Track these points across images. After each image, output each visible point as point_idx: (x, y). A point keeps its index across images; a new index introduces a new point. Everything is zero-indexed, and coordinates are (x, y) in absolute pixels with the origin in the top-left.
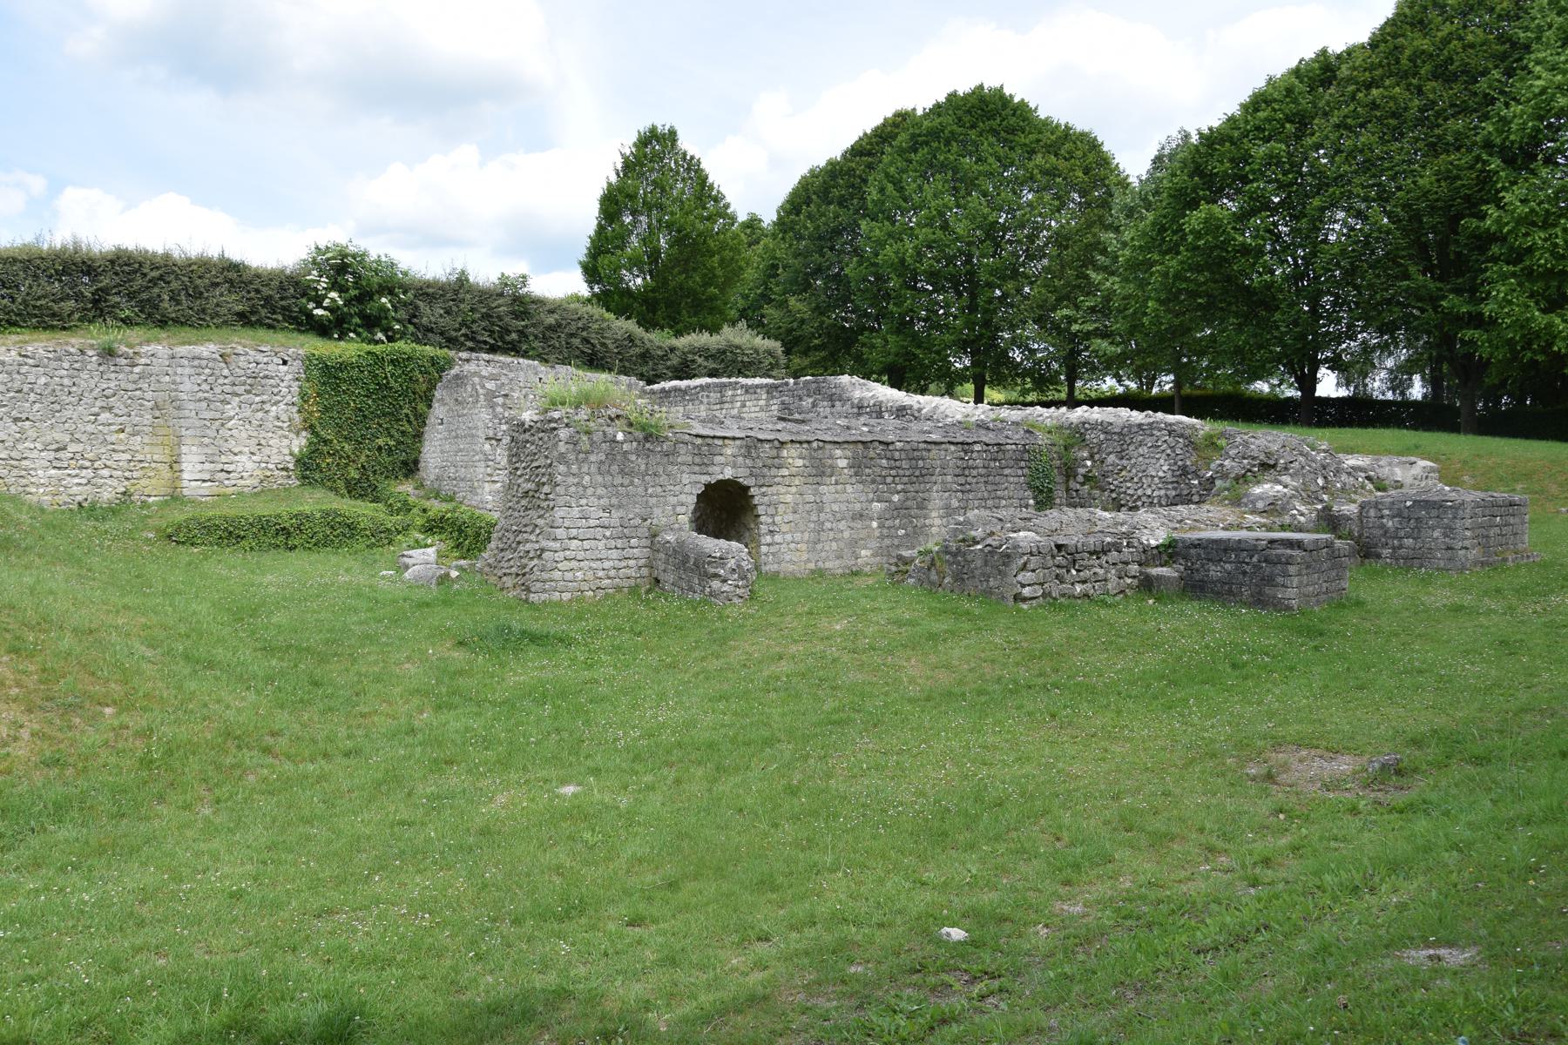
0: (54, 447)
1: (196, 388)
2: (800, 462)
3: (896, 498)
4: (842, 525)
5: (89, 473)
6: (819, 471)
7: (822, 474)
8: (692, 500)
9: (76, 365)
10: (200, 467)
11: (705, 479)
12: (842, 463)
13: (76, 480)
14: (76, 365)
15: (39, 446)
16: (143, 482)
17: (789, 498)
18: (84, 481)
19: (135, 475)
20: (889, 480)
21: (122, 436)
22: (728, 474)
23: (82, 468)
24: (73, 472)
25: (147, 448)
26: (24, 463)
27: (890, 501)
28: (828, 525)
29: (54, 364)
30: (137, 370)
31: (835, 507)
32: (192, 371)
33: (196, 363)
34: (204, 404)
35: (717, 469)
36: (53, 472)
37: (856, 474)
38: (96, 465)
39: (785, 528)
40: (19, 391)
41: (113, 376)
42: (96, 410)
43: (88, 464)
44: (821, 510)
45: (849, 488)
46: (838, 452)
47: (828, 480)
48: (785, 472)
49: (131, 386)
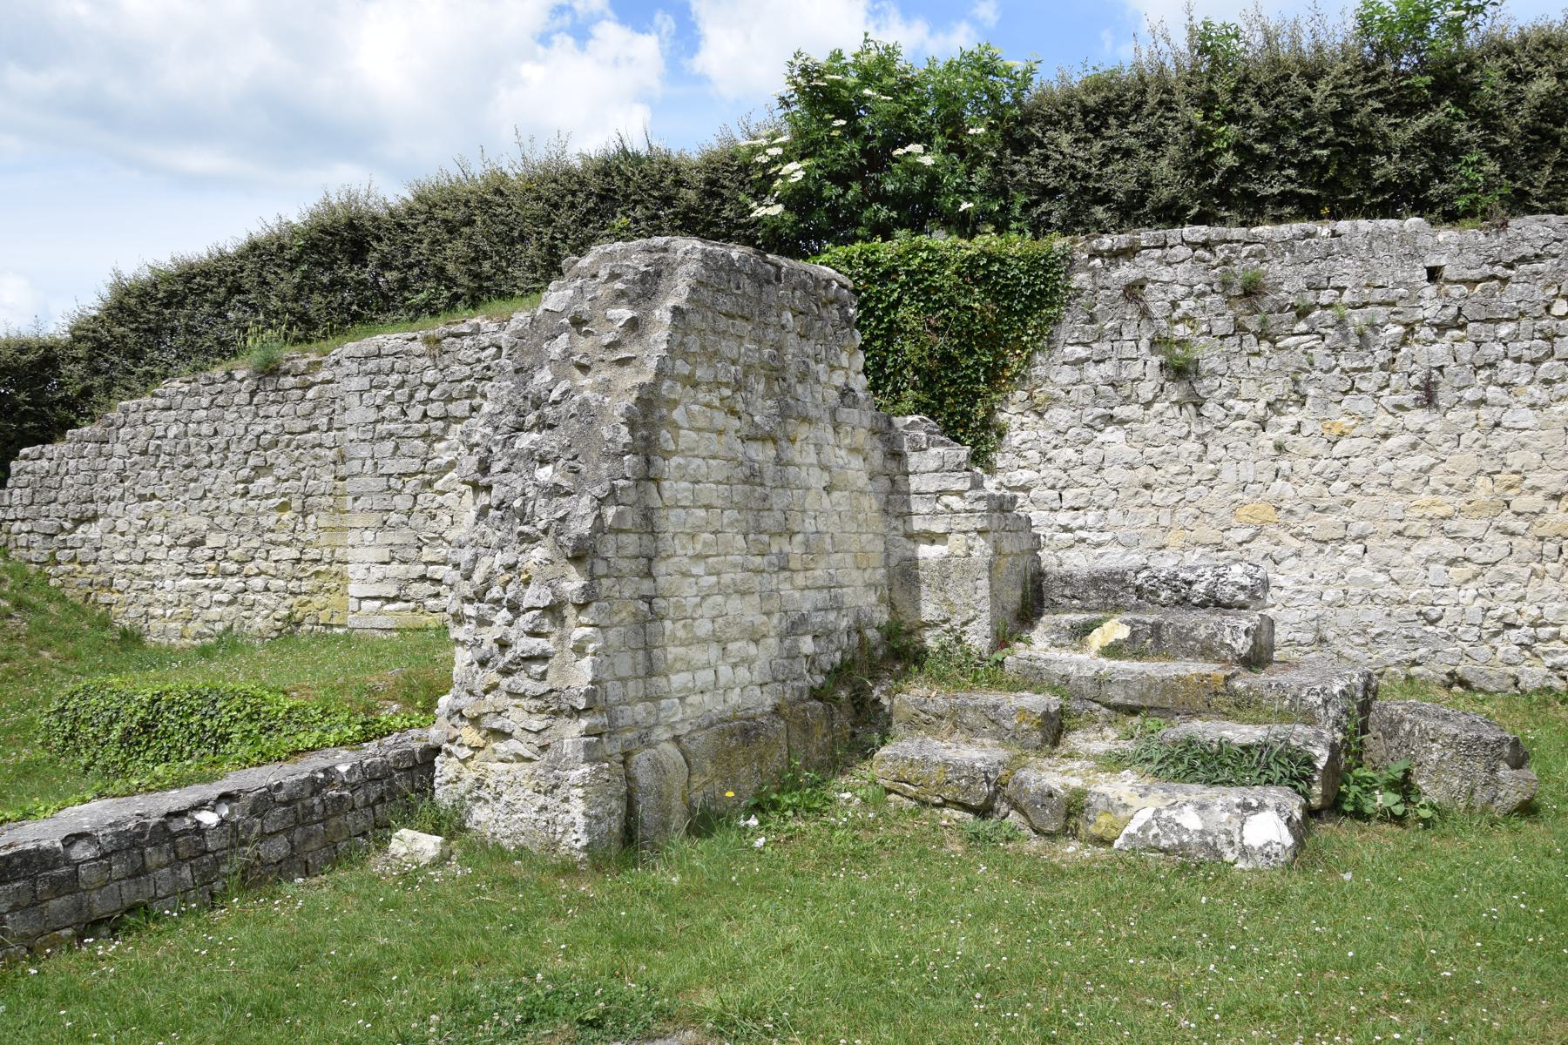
0: (186, 540)
1: (372, 415)
5: (234, 584)
9: (220, 400)
10: (378, 572)
13: (218, 596)
14: (220, 400)
15: (167, 540)
16: (318, 601)
18: (225, 598)
19: (306, 586)
21: (286, 516)
23: (225, 575)
24: (213, 582)
25: (324, 536)
26: (149, 567)
29: (190, 402)
30: (311, 394)
32: (364, 382)
33: (372, 365)
34: (389, 445)
36: (188, 580)
38: (250, 568)
40: (144, 453)
41: (273, 409)
42: (245, 472)
43: (233, 567)
49: (301, 425)
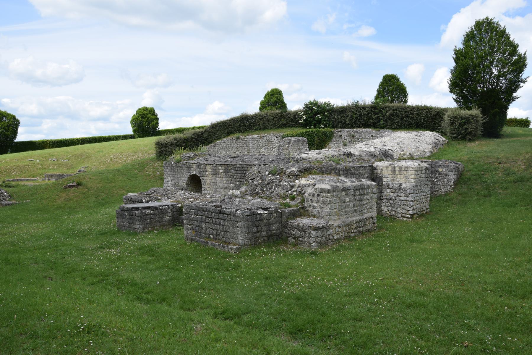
2: (210, 170)
3: (238, 183)
4: (222, 190)
6: (216, 173)
7: (216, 174)
8: (186, 179)
11: (190, 174)
12: (221, 171)
17: (208, 181)
20: (235, 177)
22: (194, 173)
27: (235, 184)
28: (218, 190)
31: (220, 184)
35: (192, 171)
37: (225, 175)
39: (208, 189)
44: (216, 185)
45: (224, 179)
46: (220, 168)
47: (218, 176)
48: (207, 173)
